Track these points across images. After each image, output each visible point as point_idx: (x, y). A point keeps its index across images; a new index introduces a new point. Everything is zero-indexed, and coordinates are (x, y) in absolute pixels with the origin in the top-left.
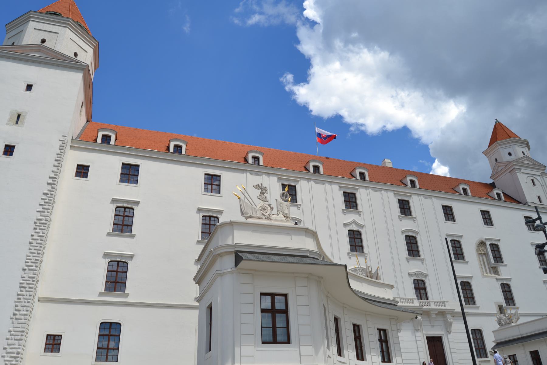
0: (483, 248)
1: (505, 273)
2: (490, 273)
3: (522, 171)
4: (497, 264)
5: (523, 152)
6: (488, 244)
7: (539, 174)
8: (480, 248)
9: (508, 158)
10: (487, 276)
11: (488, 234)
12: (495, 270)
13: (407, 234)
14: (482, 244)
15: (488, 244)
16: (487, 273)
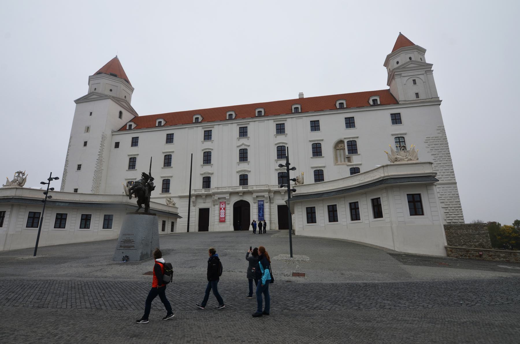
0: (342, 145)
1: (356, 160)
2: (345, 161)
3: (403, 75)
4: (350, 155)
5: (410, 58)
6: (346, 141)
7: (423, 72)
8: (340, 145)
9: (396, 66)
10: (339, 165)
11: (349, 134)
12: (349, 159)
13: (279, 145)
14: (341, 142)
15: (346, 141)
16: (341, 162)
